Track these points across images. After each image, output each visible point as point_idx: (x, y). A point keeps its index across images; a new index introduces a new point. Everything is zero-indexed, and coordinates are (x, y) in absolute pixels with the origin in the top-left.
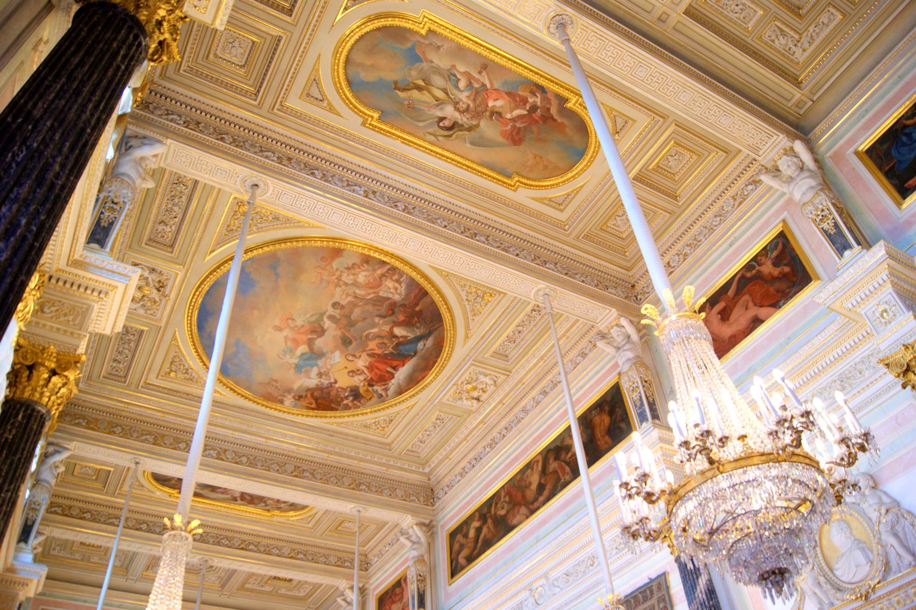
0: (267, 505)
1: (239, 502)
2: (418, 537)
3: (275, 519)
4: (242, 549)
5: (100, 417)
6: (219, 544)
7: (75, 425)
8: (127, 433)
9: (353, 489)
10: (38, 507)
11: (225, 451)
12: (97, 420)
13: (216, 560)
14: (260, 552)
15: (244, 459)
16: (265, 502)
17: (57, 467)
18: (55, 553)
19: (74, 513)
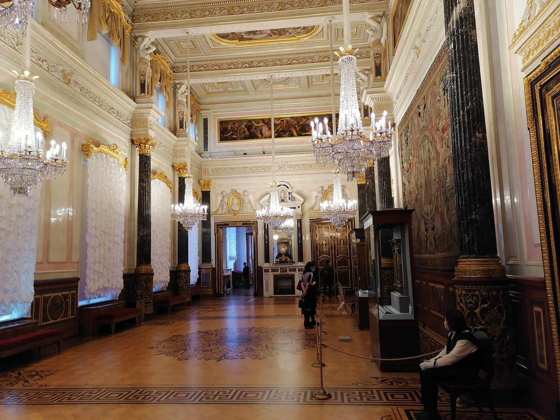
0: (290, 33)
1: (274, 36)
2: (375, 27)
3: (301, 40)
4: (289, 64)
5: (158, 12)
6: (275, 65)
7: (147, 21)
8: (175, 16)
9: (322, 6)
10: (144, 73)
11: (233, 7)
12: (157, 14)
13: (277, 74)
14: (300, 63)
15: (245, 9)
16: (288, 32)
17: (148, 49)
18: (210, 91)
19: (196, 69)
